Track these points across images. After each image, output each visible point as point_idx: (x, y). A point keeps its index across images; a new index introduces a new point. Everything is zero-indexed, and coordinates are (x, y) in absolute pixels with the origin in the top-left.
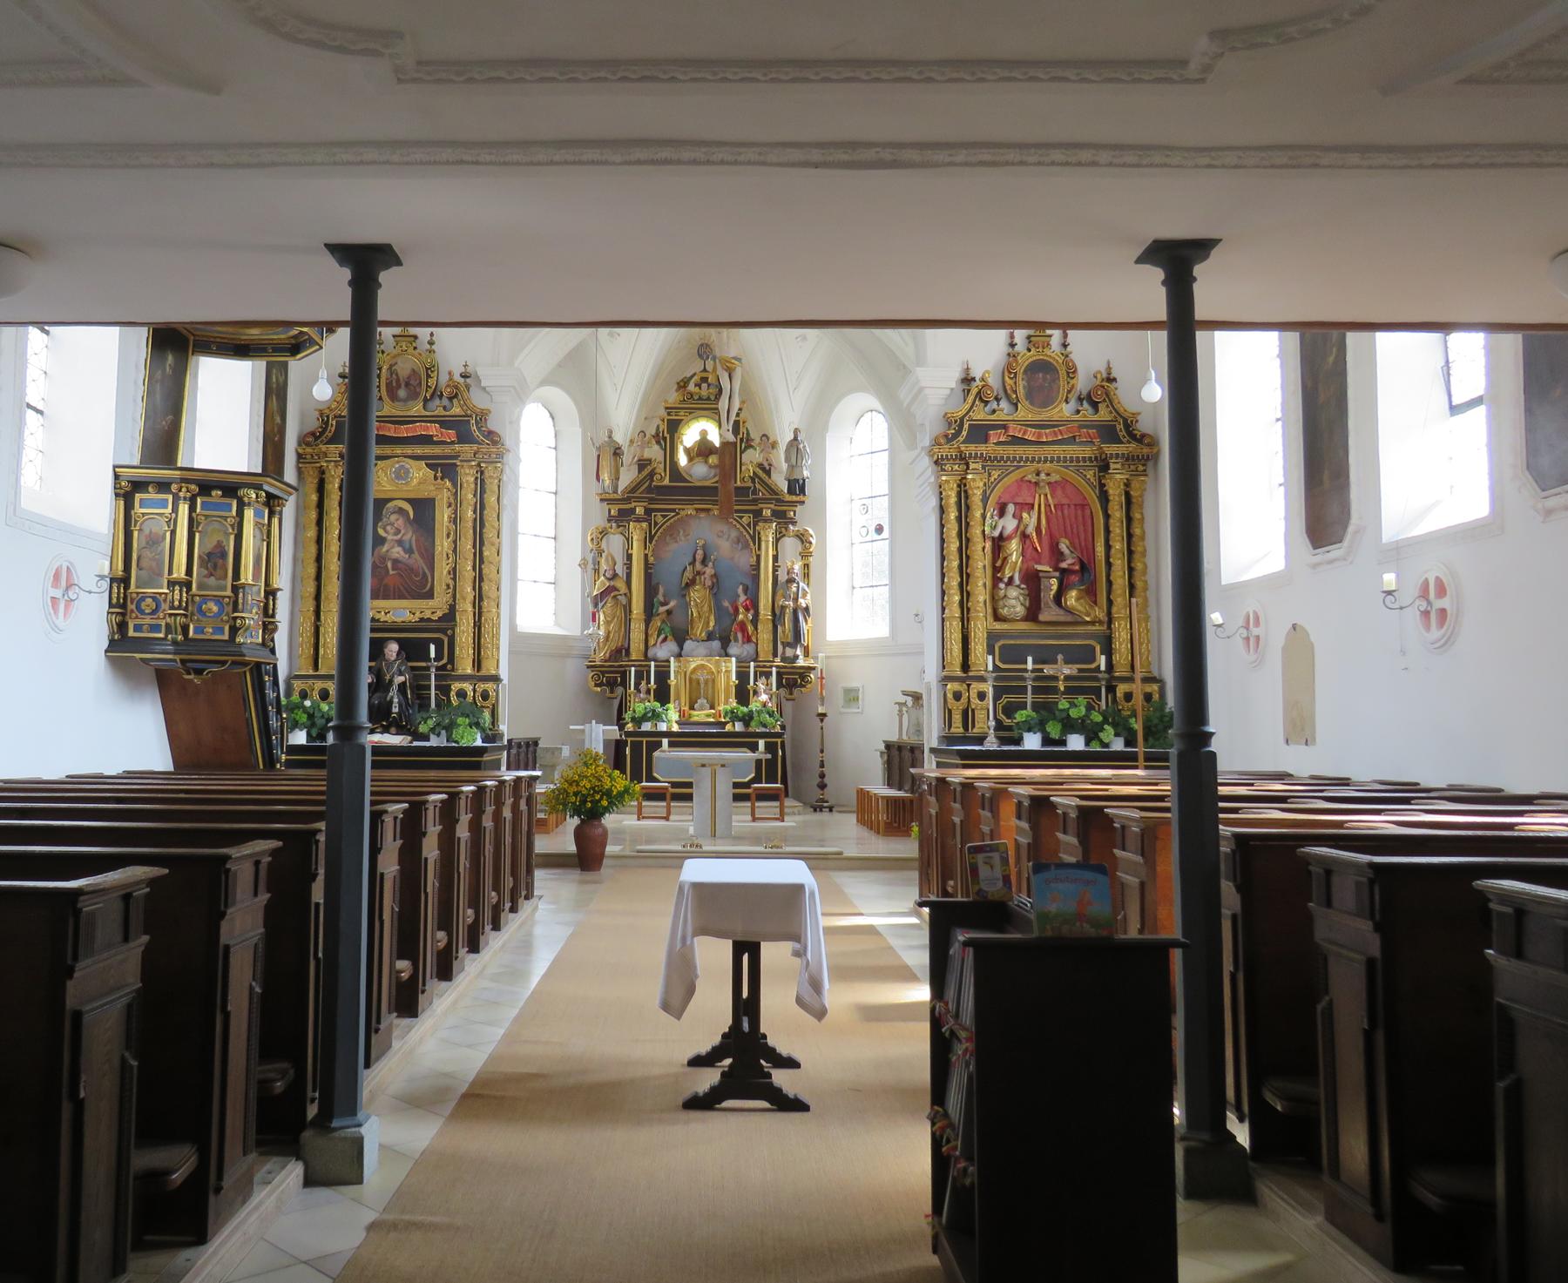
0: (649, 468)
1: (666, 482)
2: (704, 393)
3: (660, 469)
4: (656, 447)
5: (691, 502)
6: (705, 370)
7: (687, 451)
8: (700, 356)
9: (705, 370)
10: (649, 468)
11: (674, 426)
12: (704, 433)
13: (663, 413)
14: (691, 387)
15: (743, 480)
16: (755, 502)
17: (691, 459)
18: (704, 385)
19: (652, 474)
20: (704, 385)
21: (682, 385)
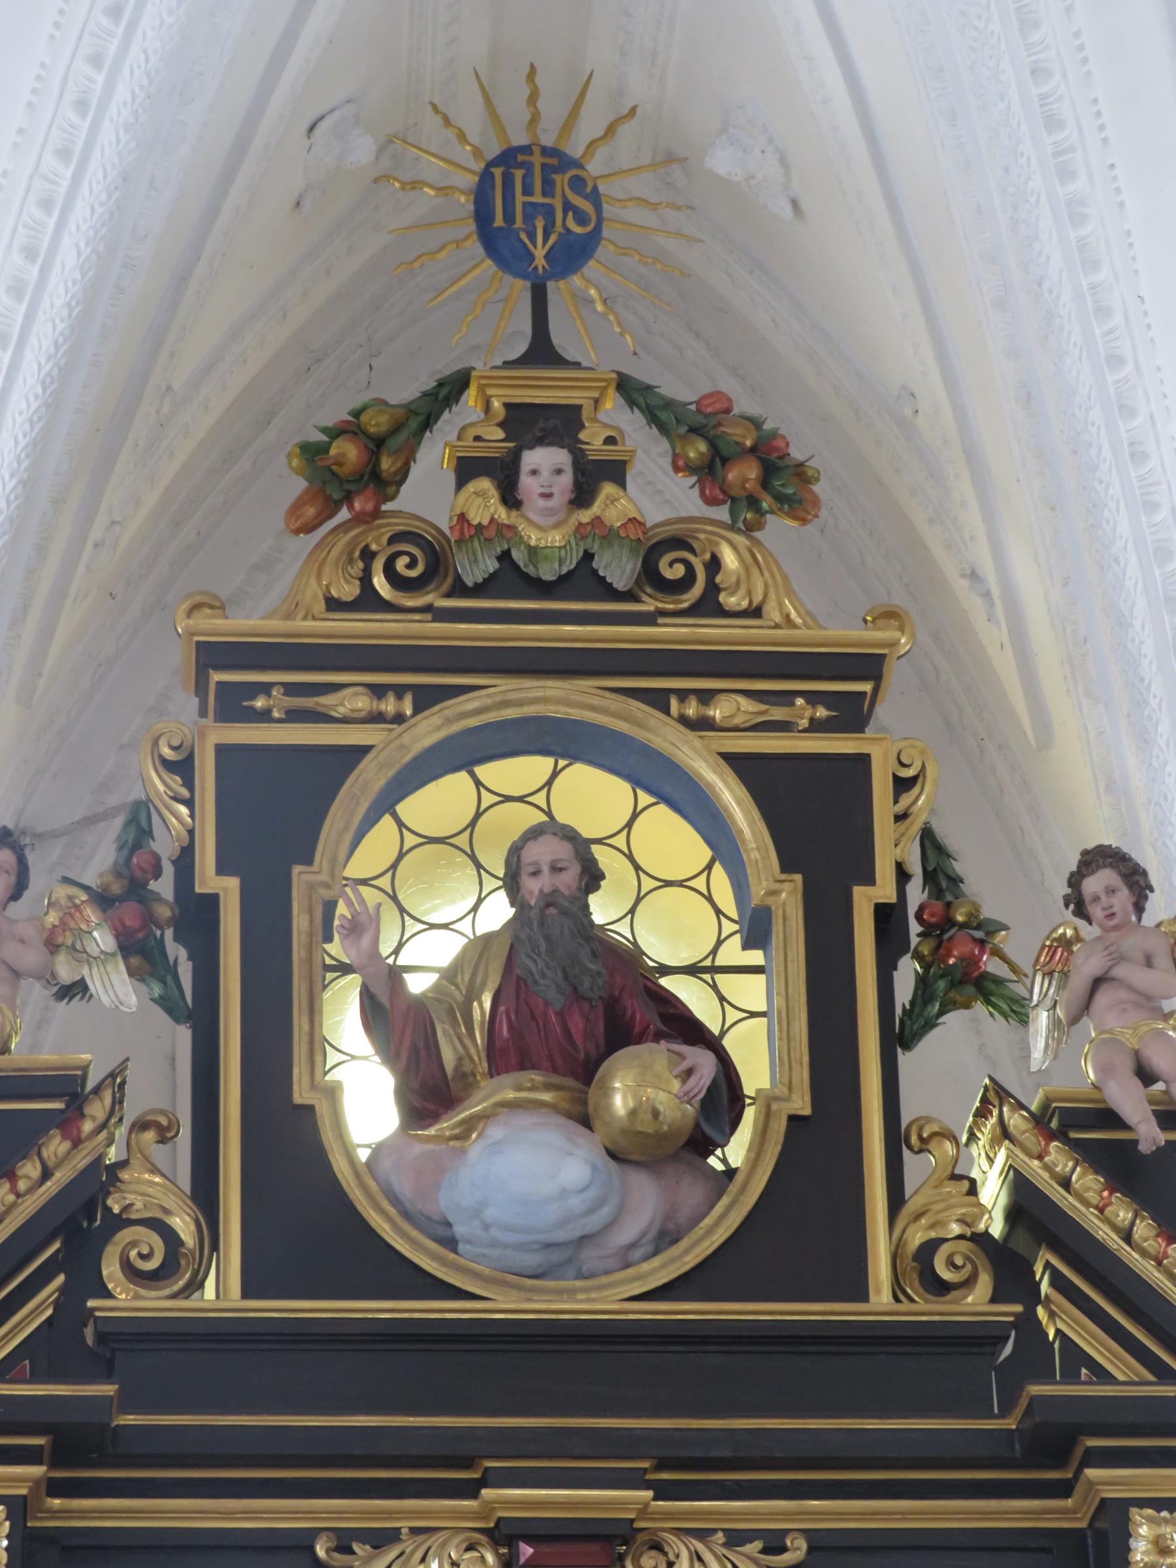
0: (60, 1160)
1: (220, 1291)
2: (546, 533)
3: (154, 1186)
4: (117, 988)
5: (451, 1468)
6: (542, 352)
7: (398, 1022)
8: (497, 240)
9: (542, 352)
10: (60, 1160)
11: (280, 812)
12: (555, 882)
13: (183, 718)
14: (429, 492)
15: (919, 1270)
16: (1051, 1448)
17: (429, 1095)
18: (545, 465)
19: (81, 1222)
20: (545, 465)
21: (352, 468)
